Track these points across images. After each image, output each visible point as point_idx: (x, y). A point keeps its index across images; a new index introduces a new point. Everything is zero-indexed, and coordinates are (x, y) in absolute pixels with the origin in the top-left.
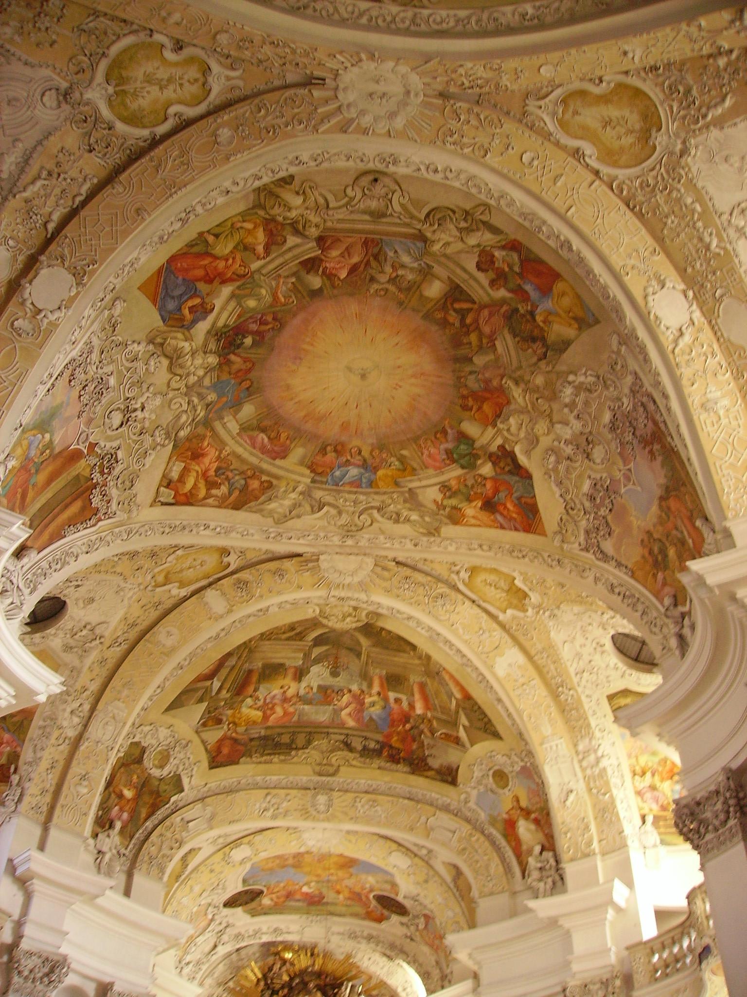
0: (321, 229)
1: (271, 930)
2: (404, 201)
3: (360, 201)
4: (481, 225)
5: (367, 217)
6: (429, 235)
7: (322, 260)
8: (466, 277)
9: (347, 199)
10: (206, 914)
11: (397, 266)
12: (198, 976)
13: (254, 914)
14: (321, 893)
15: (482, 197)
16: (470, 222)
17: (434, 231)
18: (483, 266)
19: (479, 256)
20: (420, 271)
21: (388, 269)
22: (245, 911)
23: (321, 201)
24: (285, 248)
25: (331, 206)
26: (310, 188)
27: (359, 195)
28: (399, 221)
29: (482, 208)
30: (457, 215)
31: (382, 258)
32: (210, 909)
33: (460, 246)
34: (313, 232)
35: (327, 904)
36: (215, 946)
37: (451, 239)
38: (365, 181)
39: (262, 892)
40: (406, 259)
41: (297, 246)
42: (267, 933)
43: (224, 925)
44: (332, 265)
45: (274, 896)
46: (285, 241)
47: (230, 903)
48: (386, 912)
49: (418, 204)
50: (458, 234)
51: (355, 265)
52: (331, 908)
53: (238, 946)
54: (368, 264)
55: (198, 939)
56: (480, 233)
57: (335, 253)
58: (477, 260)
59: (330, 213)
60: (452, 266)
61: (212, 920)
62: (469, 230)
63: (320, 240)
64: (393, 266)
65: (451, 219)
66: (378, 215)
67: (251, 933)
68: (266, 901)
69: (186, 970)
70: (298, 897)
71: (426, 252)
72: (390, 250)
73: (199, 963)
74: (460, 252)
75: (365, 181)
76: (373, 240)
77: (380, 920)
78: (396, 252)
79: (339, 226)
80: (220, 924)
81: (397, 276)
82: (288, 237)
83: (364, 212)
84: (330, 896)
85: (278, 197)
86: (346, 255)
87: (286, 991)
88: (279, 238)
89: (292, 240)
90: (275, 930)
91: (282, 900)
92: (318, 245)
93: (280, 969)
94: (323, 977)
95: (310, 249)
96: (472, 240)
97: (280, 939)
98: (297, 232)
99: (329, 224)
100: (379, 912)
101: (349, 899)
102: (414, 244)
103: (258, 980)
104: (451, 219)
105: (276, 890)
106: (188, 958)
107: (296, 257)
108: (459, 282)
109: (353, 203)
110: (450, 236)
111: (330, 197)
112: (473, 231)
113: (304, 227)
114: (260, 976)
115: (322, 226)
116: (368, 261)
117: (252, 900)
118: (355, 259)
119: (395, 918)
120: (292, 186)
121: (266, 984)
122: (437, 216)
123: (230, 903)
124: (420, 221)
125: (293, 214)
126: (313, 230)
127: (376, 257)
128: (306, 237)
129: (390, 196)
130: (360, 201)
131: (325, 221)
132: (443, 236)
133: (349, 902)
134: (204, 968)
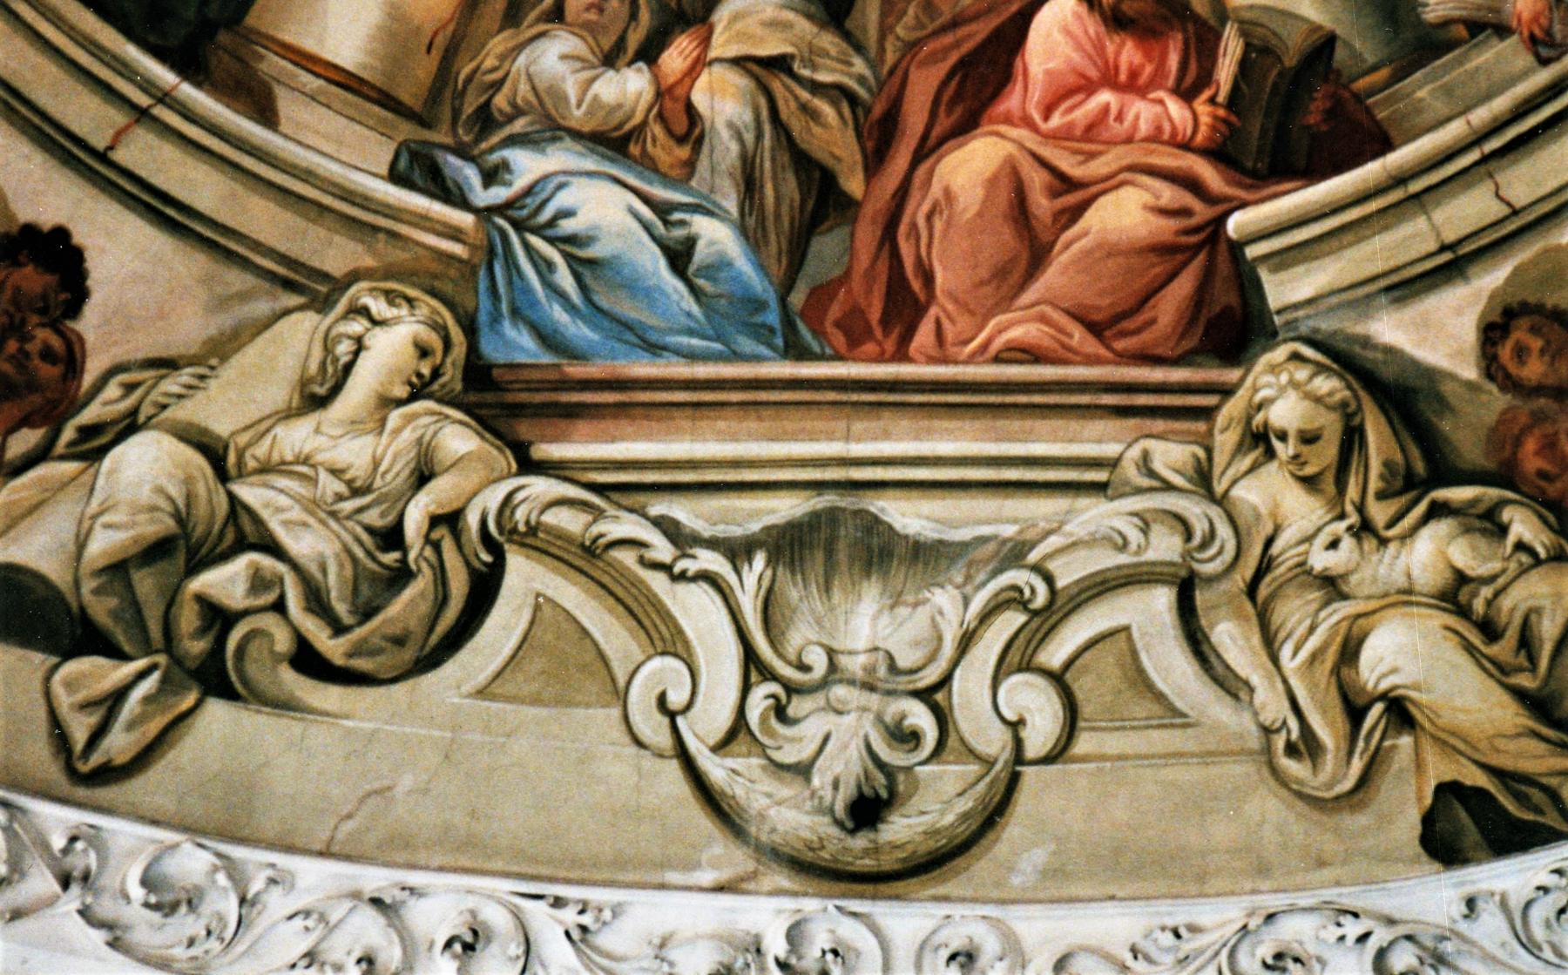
0: (1233, 408)
2: (663, 672)
3: (966, 642)
4: (101, 609)
5: (908, 516)
6: (459, 439)
7: (1217, 154)
8: (146, 155)
9: (1055, 654)
11: (666, 152)
15: (123, 833)
16: (188, 619)
17: (422, 476)
18: (31, 279)
19: (72, 358)
20: (485, 120)
21: (723, 102)
23: (1232, 638)
24: (1491, 279)
25: (1163, 599)
26: (1307, 746)
27: (970, 687)
28: (681, 510)
29: (119, 744)
30: (283, 641)
31: (782, 191)
33: (221, 407)
34: (1284, 390)
37: (296, 437)
38: (936, 802)
40: (602, 207)
41: (1406, 286)
44: (1142, 113)
46: (1493, 332)
49: (563, 667)
50: (248, 493)
51: (966, 126)
54: (879, 135)
56: (102, 545)
57: (1126, 213)
58: (88, 324)
59: (1165, 547)
60: (261, 219)
62: (181, 547)
63: (1234, 327)
64: (690, 129)
65: (317, 602)
66: (834, 541)
71: (464, 289)
72: (719, 266)
74: (221, 349)
75: (936, 802)
76: (855, 338)
78: (679, 256)
79: (1096, 440)
81: (649, 53)
82: (1470, 372)
83: (928, 557)
85: (1537, 704)
86: (1042, 205)
88: (1533, 370)
89: (1438, 335)
92: (1247, 284)
95: (1312, 249)
96: (146, 472)
98: (1400, 393)
99: (1171, 455)
102: (548, 338)
104: (317, 602)
107: (1410, 195)
108: (188, 92)
109: (1012, 621)
110: (301, 467)
111: (1171, 665)
112: (155, 551)
113: (1352, 438)
115: (1224, 441)
116: (875, 161)
118: (970, 167)
120: (1441, 769)
122: (412, 604)
124: (534, 539)
125: (1430, 552)
126: (1286, 413)
127: (824, 201)
128: (1343, 357)
129: (760, 697)
130: (966, 642)
131: (1203, 478)
132: (355, 453)
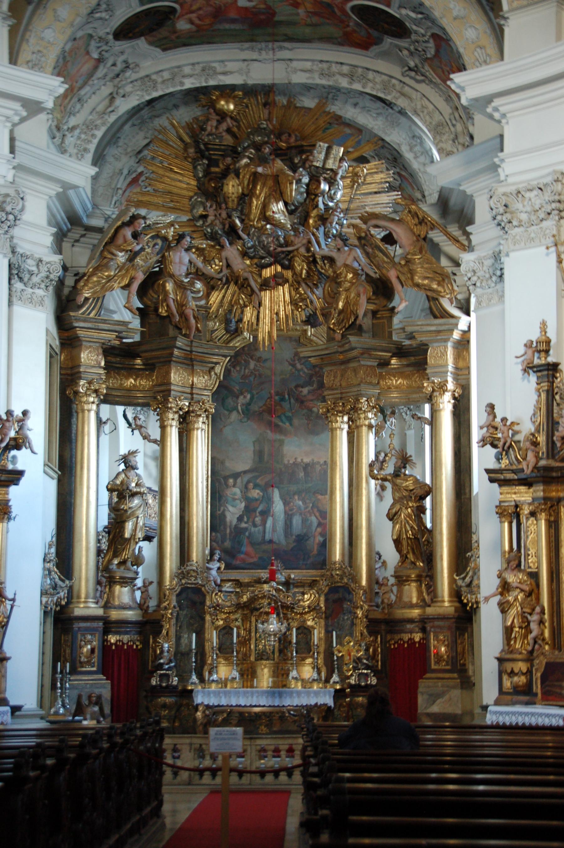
1: (198, 68)
10: (88, 53)
12: (92, 147)
13: (167, 45)
14: (269, 7)
22: (151, 43)
32: (93, 44)
35: (280, 23)
36: (112, 98)
39: (173, 10)
42: (191, 76)
43: (120, 66)
45: (193, 16)
47: (125, 32)
48: (375, 33)
52: (289, 31)
53: (148, 98)
55: (82, 92)
61: (100, 61)
67: (166, 75)
68: (183, 25)
69: (70, 140)
70: (233, 15)
73: (89, 126)
77: (364, 45)
80: (114, 65)
84: (284, 11)
87: (229, 160)
90: (203, 70)
91: (207, 21)
93: (217, 128)
94: (284, 137)
97: (212, 83)
100: (363, 33)
101: (315, 14)
103: (186, 146)
105: (194, 8)
106: (73, 121)
114: (187, 139)
117: (160, 24)
119: (388, 41)
121: (199, 151)
123: (125, 32)
133: (315, 20)
134: (99, 134)
